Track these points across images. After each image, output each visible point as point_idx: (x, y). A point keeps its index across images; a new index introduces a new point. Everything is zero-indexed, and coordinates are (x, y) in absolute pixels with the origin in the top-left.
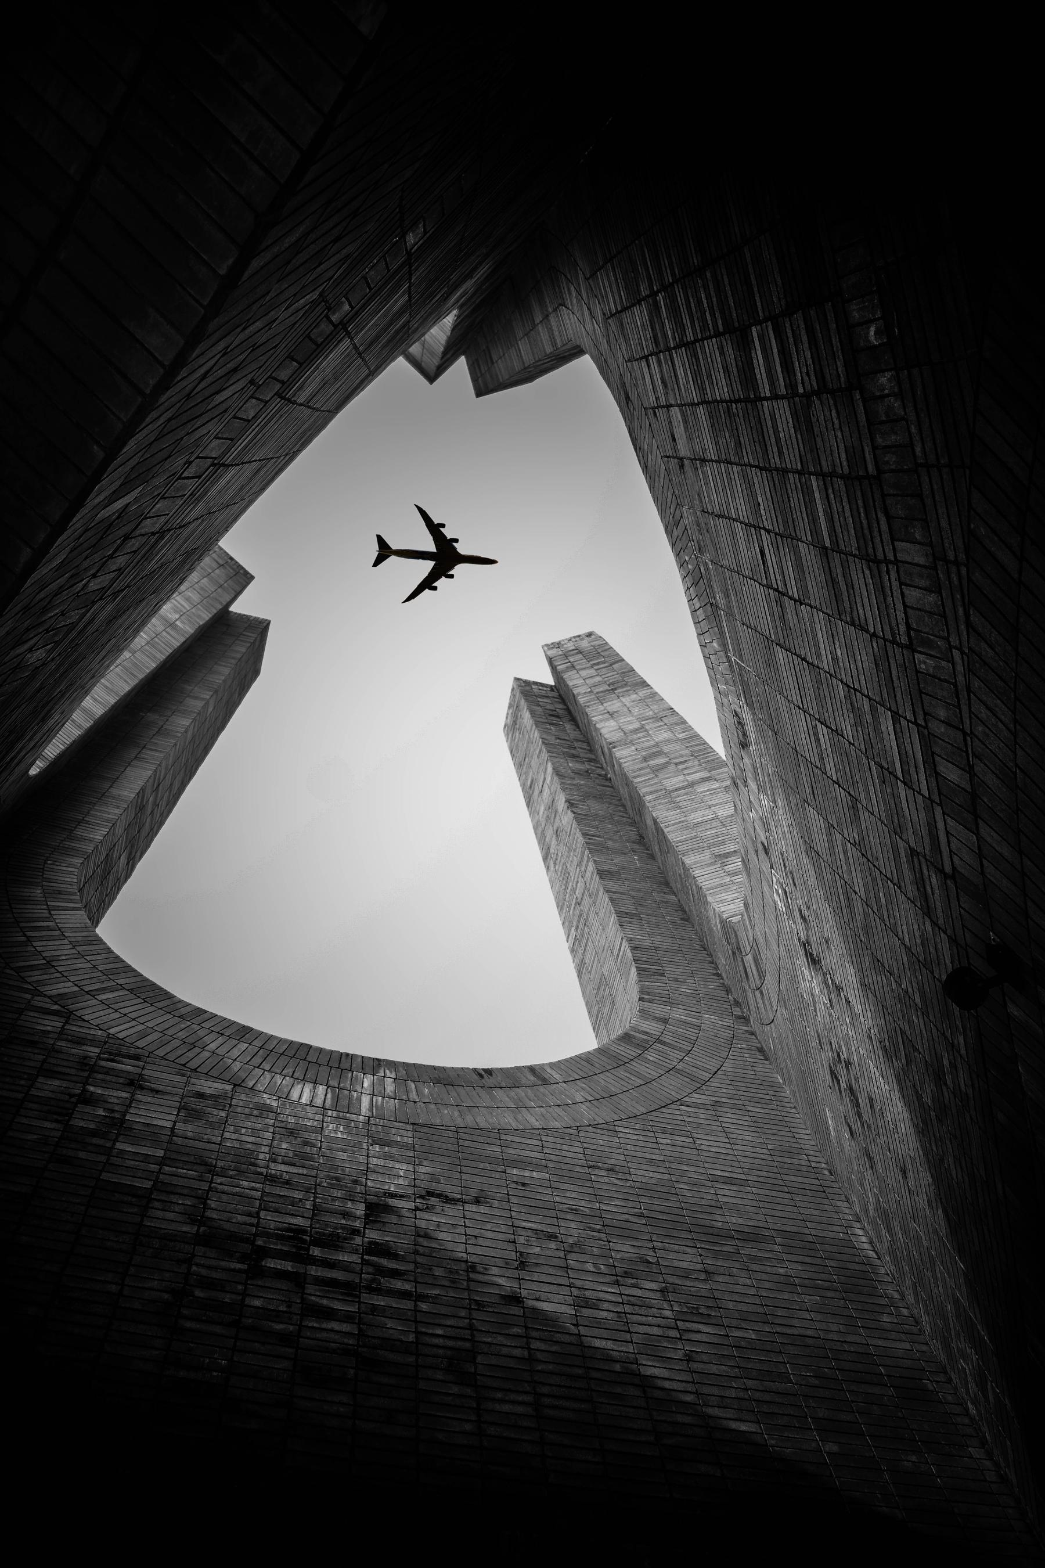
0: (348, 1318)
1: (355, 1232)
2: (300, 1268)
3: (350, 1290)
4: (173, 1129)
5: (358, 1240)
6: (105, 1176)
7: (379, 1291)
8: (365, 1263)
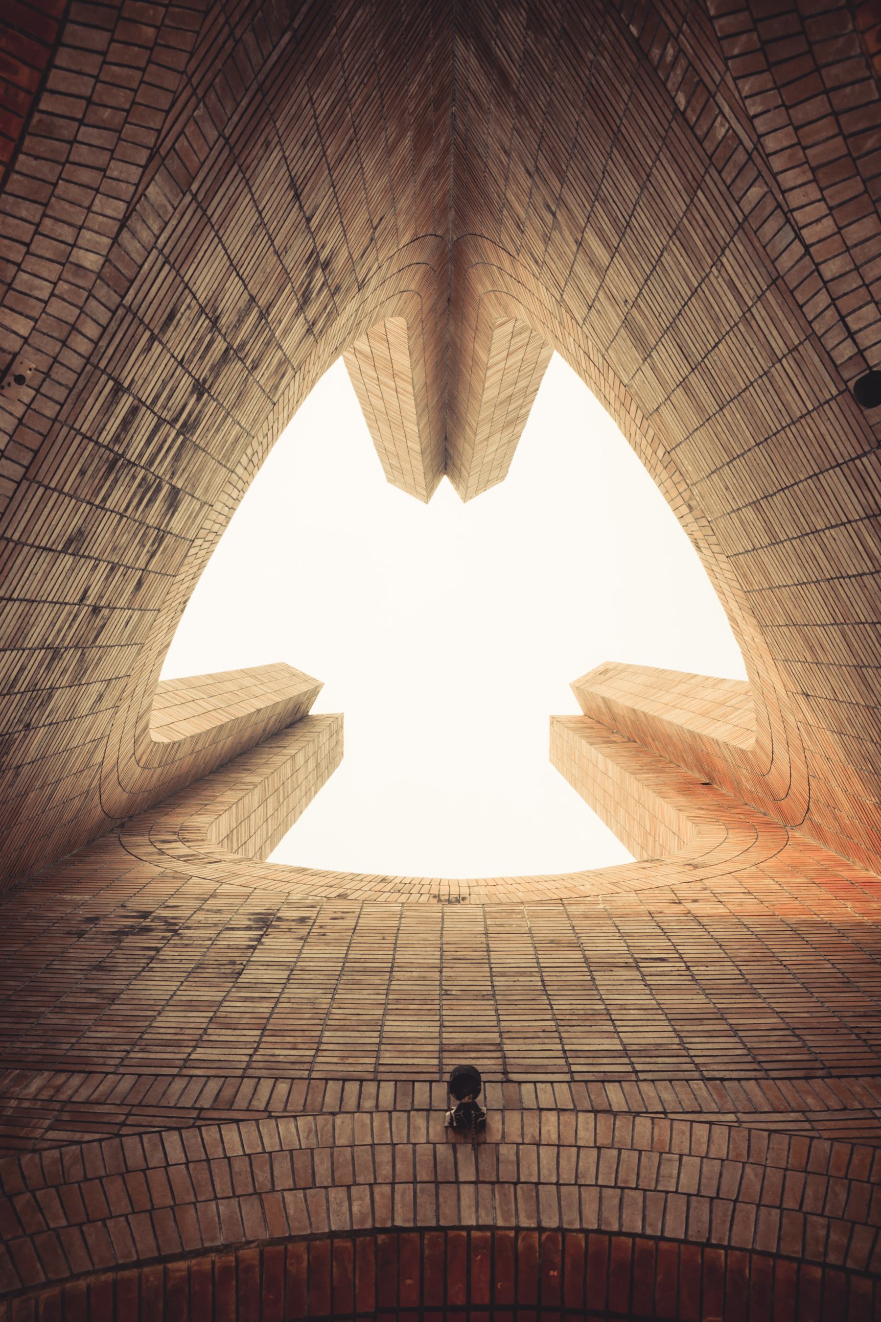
0: (141, 455)
1: (171, 478)
2: (178, 426)
3: (151, 462)
4: (280, 347)
5: (167, 478)
6: (290, 285)
7: (139, 486)
8: (157, 477)
